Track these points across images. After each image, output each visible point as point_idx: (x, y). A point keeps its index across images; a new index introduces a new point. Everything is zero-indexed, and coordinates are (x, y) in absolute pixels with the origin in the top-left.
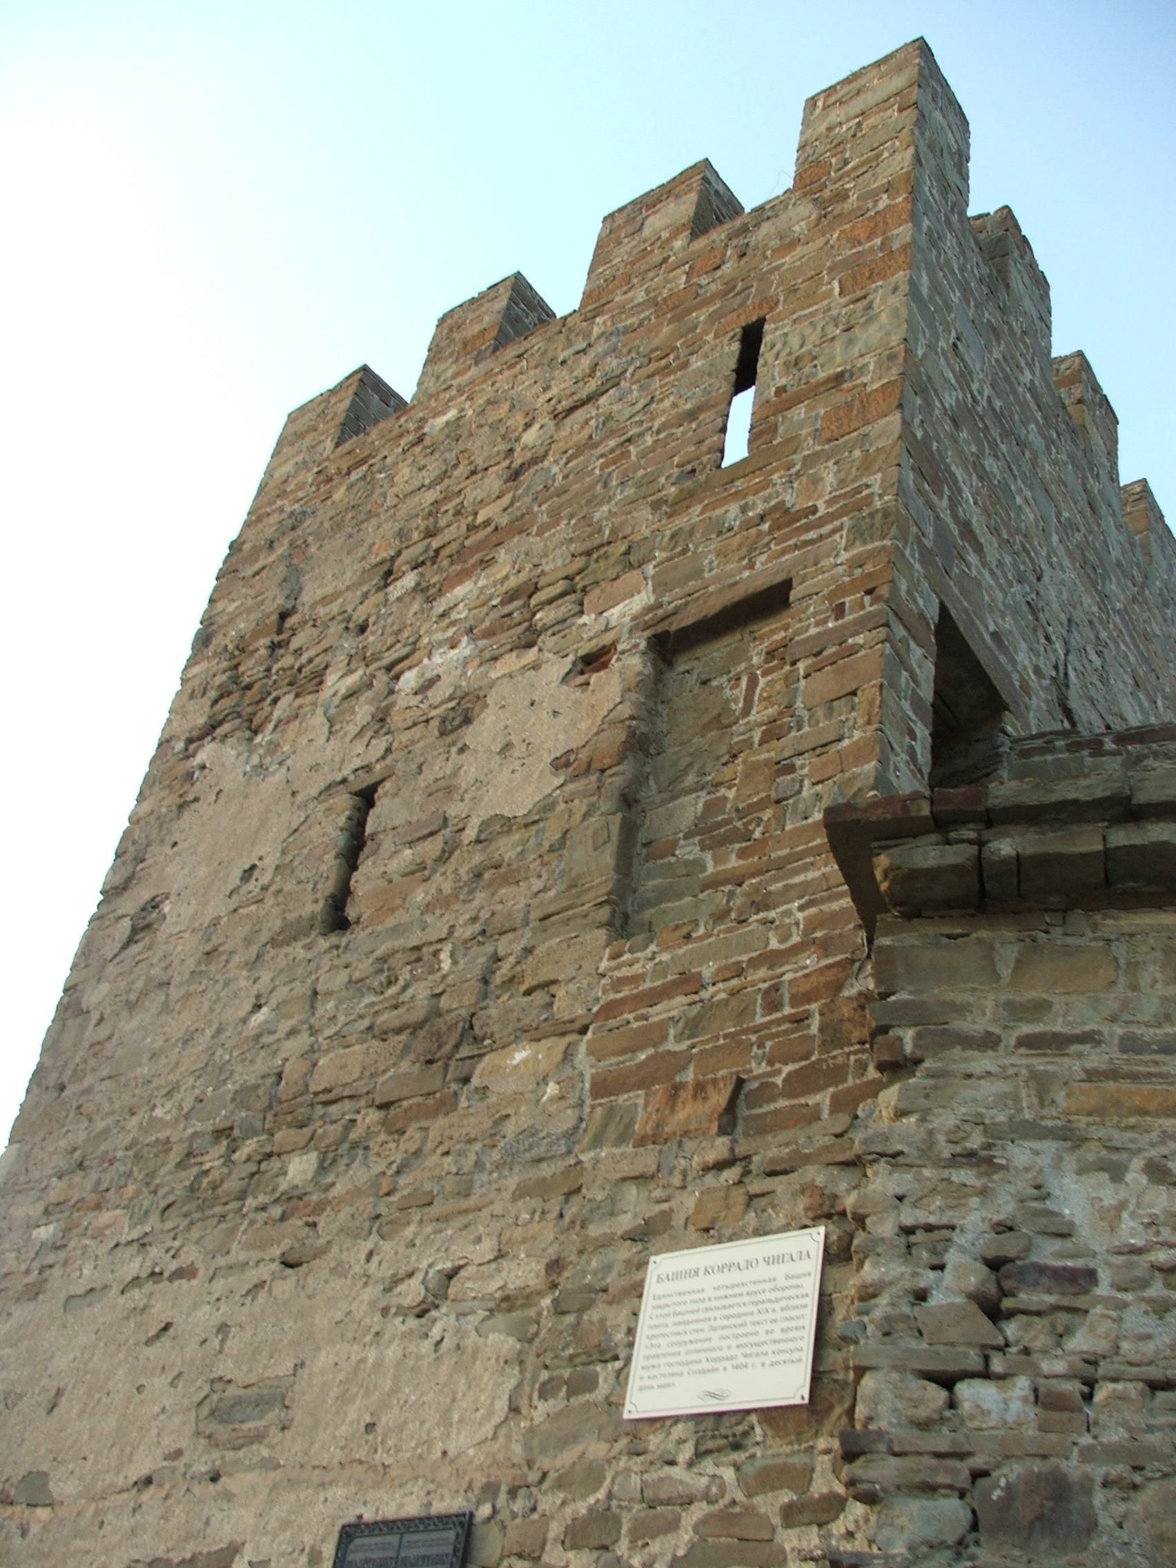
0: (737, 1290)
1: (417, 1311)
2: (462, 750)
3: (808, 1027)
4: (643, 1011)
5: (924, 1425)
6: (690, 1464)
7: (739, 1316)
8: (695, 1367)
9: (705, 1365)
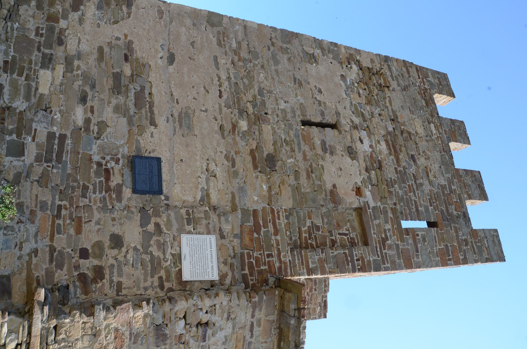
1: (208, 169)
2: (342, 156)
3: (263, 266)
4: (271, 221)
5: (176, 314)
6: (171, 253)
8: (191, 252)
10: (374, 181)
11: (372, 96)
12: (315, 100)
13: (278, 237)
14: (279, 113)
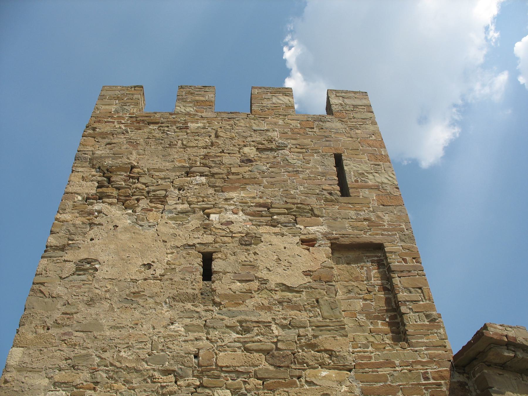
10: (291, 218)
11: (148, 192)
12: (166, 277)
13: (397, 362)
14: (191, 336)
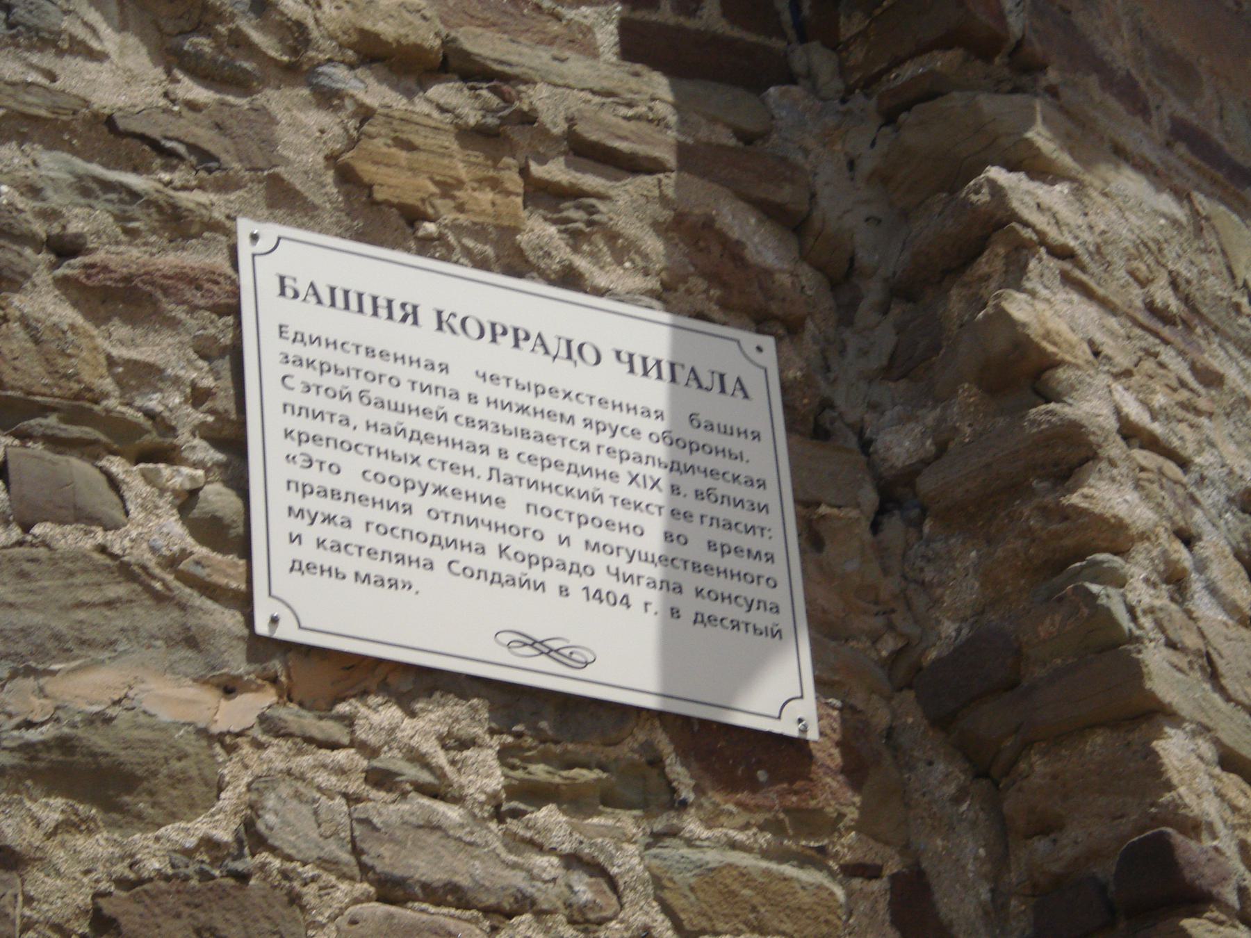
0: (546, 402)
7: (572, 469)
9: (491, 562)
